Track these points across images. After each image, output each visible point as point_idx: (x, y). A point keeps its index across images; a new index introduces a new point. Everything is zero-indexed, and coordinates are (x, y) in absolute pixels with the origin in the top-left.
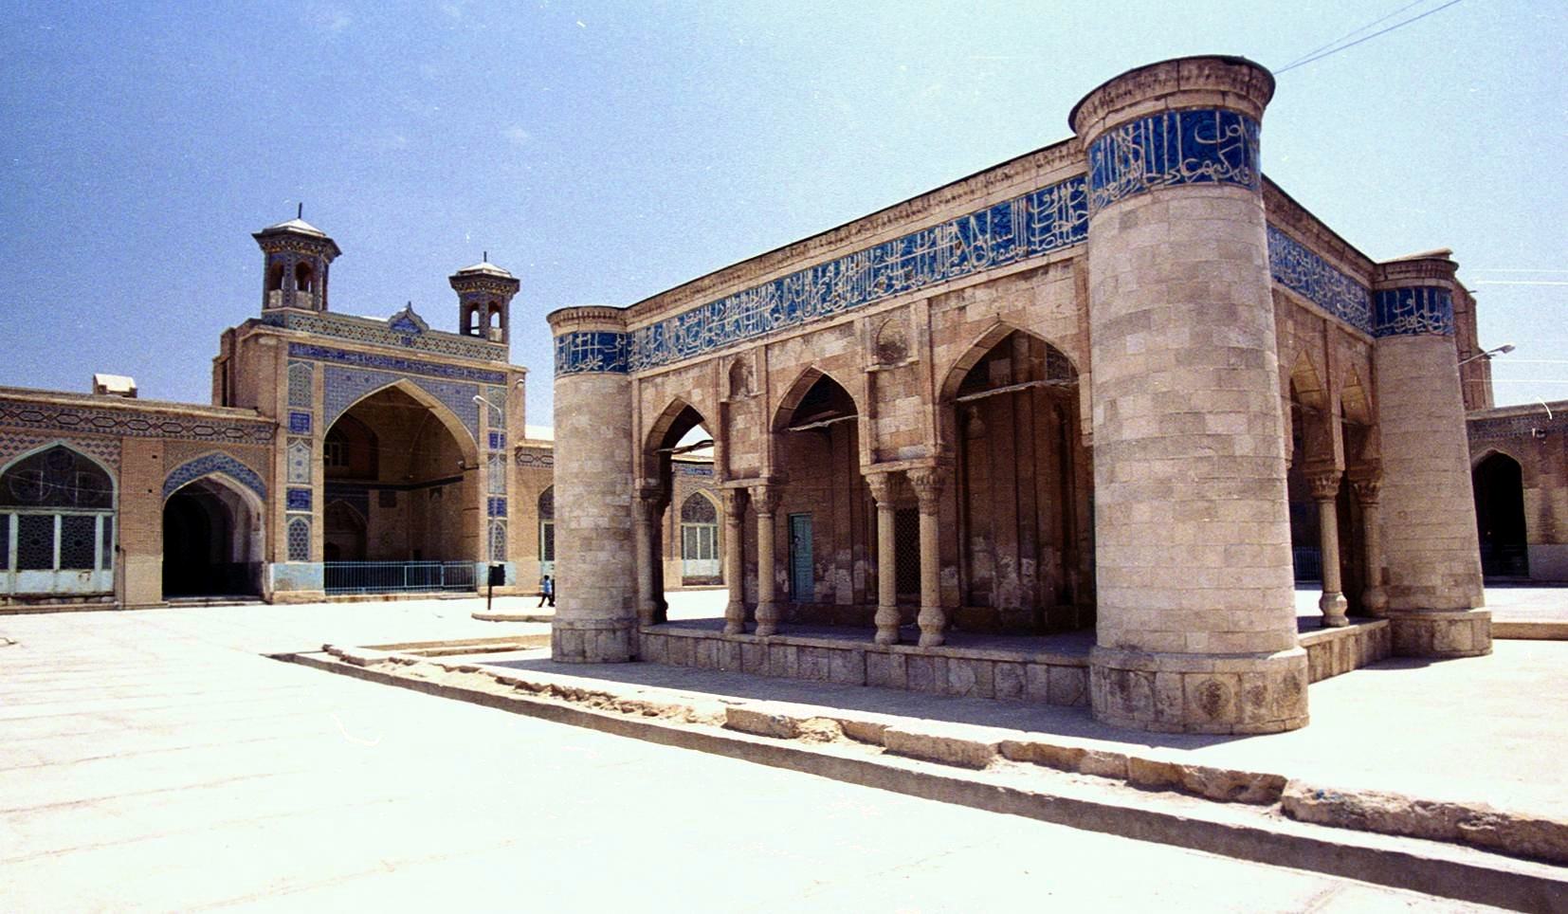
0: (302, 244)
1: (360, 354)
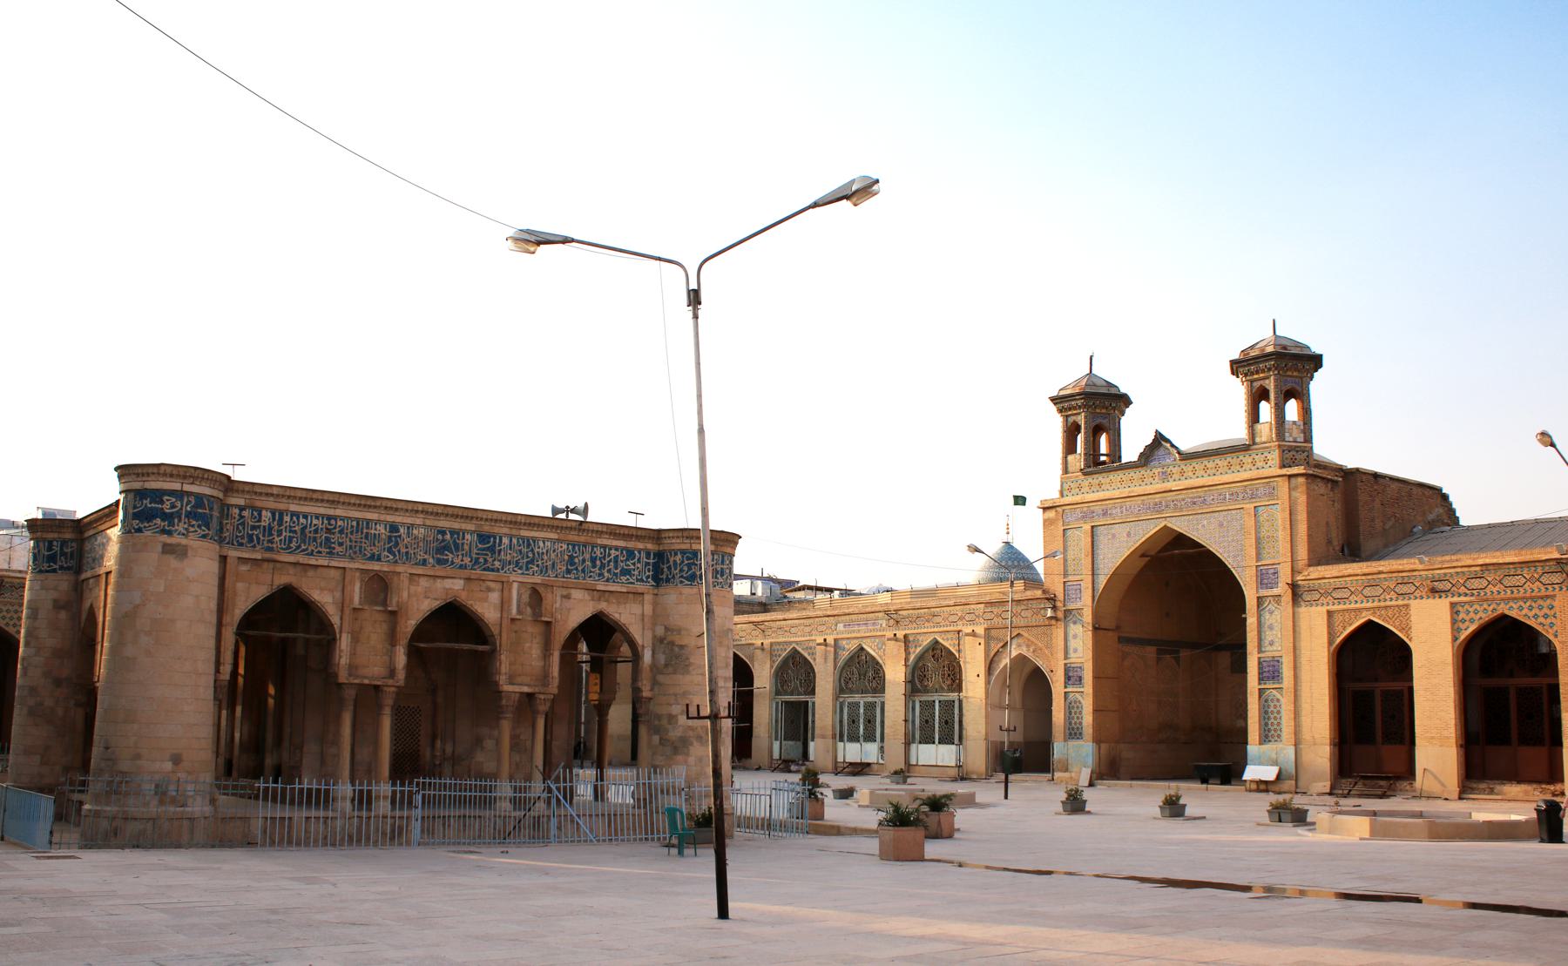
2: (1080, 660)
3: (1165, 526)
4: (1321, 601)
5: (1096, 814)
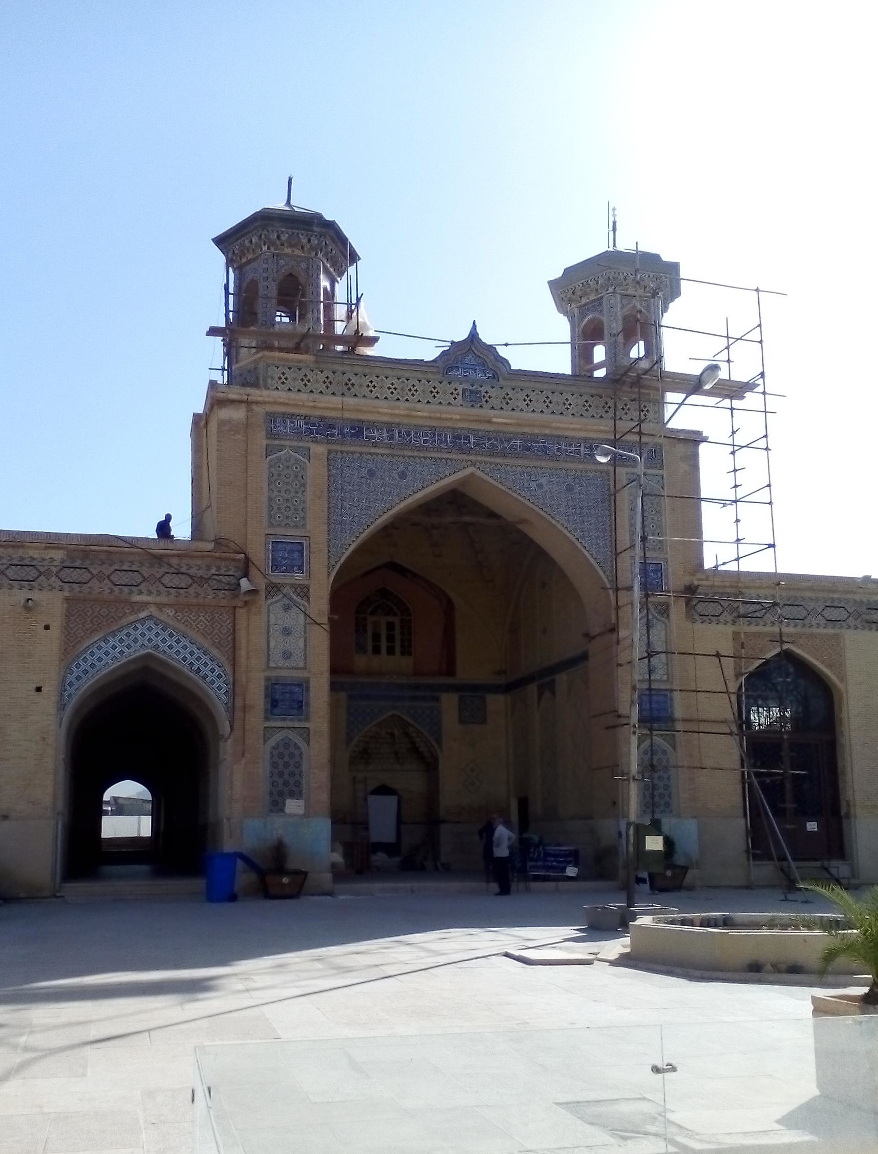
0: (284, 238)
1: (390, 427)
2: (295, 674)
3: (472, 474)
4: (721, 618)
5: (539, 939)
